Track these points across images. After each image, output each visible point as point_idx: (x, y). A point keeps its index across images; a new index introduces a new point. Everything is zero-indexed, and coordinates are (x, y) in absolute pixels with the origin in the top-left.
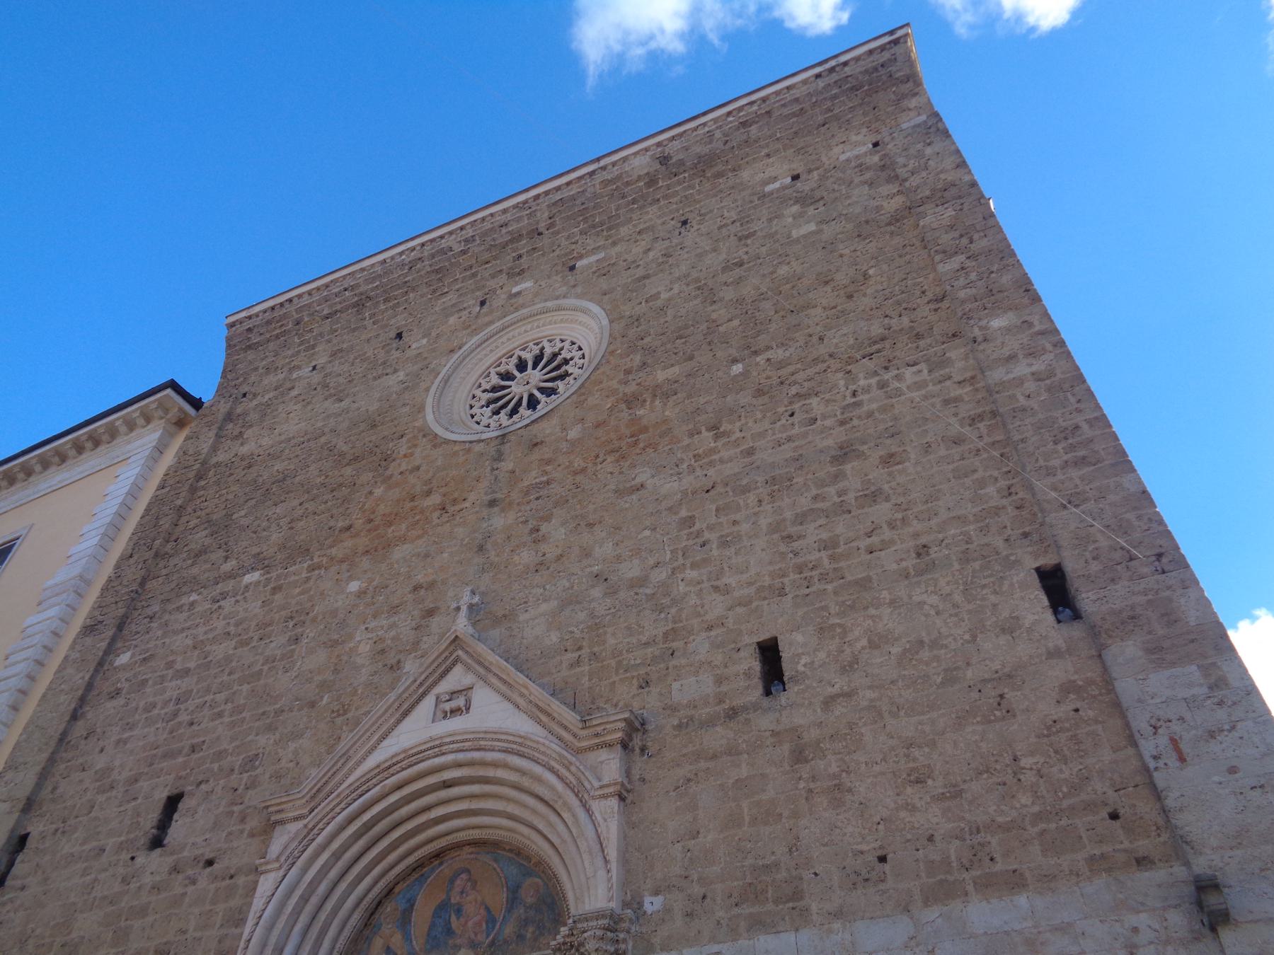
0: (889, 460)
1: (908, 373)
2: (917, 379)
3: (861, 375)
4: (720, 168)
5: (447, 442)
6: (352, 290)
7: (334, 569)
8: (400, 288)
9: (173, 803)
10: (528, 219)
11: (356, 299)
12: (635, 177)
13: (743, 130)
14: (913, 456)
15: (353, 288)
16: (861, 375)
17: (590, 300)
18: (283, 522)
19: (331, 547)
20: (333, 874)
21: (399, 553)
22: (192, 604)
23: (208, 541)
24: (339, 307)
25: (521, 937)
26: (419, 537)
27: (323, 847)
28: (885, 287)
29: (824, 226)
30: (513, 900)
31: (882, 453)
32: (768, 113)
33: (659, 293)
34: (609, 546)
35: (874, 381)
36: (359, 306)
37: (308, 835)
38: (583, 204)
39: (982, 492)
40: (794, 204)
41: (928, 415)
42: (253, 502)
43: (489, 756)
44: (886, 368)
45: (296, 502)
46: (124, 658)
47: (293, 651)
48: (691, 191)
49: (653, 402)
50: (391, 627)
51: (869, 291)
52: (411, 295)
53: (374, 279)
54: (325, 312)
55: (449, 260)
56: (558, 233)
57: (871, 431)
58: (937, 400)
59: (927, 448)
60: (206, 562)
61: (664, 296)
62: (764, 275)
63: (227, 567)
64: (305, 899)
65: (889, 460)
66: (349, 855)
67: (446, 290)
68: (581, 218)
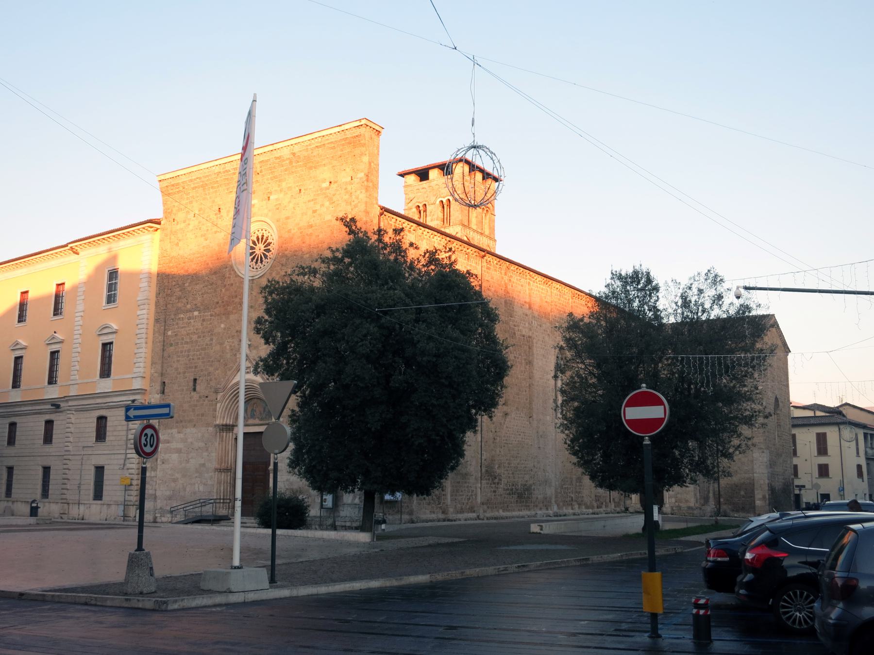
5: (239, 276)
7: (217, 317)
8: (215, 184)
9: (195, 380)
11: (202, 183)
12: (285, 158)
15: (200, 178)
17: (273, 222)
18: (200, 293)
19: (215, 309)
20: (231, 404)
21: (232, 317)
22: (183, 318)
24: (196, 185)
25: (266, 418)
26: (236, 313)
27: (227, 399)
30: (264, 411)
32: (324, 145)
33: (291, 229)
36: (204, 186)
37: (224, 396)
42: (189, 281)
43: (255, 385)
45: (202, 286)
46: (170, 333)
47: (212, 343)
50: (233, 342)
52: (220, 188)
53: (205, 177)
54: (192, 186)
55: (230, 175)
56: (263, 176)
60: (182, 302)
61: (293, 231)
63: (189, 306)
64: (226, 408)
66: (233, 400)
68: (270, 171)
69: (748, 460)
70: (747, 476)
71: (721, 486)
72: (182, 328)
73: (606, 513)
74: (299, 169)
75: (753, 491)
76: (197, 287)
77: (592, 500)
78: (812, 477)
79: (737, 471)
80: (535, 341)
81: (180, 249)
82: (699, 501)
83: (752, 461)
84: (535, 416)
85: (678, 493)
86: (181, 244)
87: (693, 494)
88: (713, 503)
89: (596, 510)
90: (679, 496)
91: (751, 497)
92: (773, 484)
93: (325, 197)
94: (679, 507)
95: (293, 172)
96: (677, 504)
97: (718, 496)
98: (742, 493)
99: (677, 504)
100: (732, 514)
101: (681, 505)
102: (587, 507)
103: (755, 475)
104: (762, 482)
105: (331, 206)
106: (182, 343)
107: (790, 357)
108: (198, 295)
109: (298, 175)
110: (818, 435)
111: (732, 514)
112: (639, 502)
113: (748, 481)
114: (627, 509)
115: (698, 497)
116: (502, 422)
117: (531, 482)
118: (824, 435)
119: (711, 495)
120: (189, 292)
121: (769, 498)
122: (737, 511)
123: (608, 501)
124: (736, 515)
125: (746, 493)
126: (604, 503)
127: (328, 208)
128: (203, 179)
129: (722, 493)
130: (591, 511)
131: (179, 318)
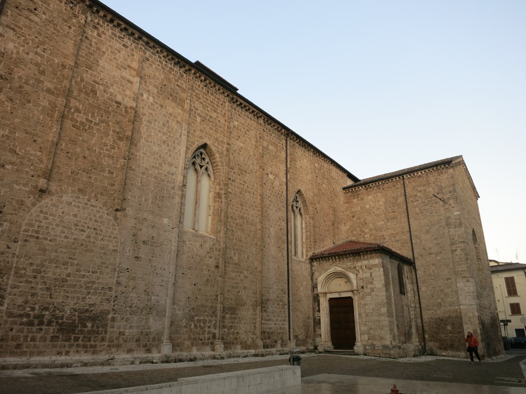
69: (452, 291)
70: (452, 308)
71: (424, 321)
73: (280, 354)
75: (461, 325)
77: (256, 338)
78: (506, 315)
79: (440, 303)
80: (145, 118)
82: (397, 338)
83: (457, 292)
84: (130, 211)
85: (371, 329)
87: (388, 328)
88: (417, 340)
89: (261, 350)
90: (372, 332)
91: (460, 332)
92: (482, 317)
94: (373, 346)
96: (370, 342)
97: (421, 331)
98: (449, 328)
99: (370, 342)
100: (439, 352)
101: (375, 343)
102: (246, 346)
103: (461, 307)
104: (471, 315)
107: (479, 201)
110: (507, 279)
111: (439, 352)
112: (330, 339)
113: (455, 314)
114: (316, 348)
115: (396, 334)
116: (28, 202)
117: (106, 307)
118: (512, 279)
119: (414, 330)
121: (481, 334)
122: (445, 349)
123: (286, 337)
124: (444, 354)
125: (453, 328)
126: (279, 342)
129: (426, 328)
130: (253, 351)
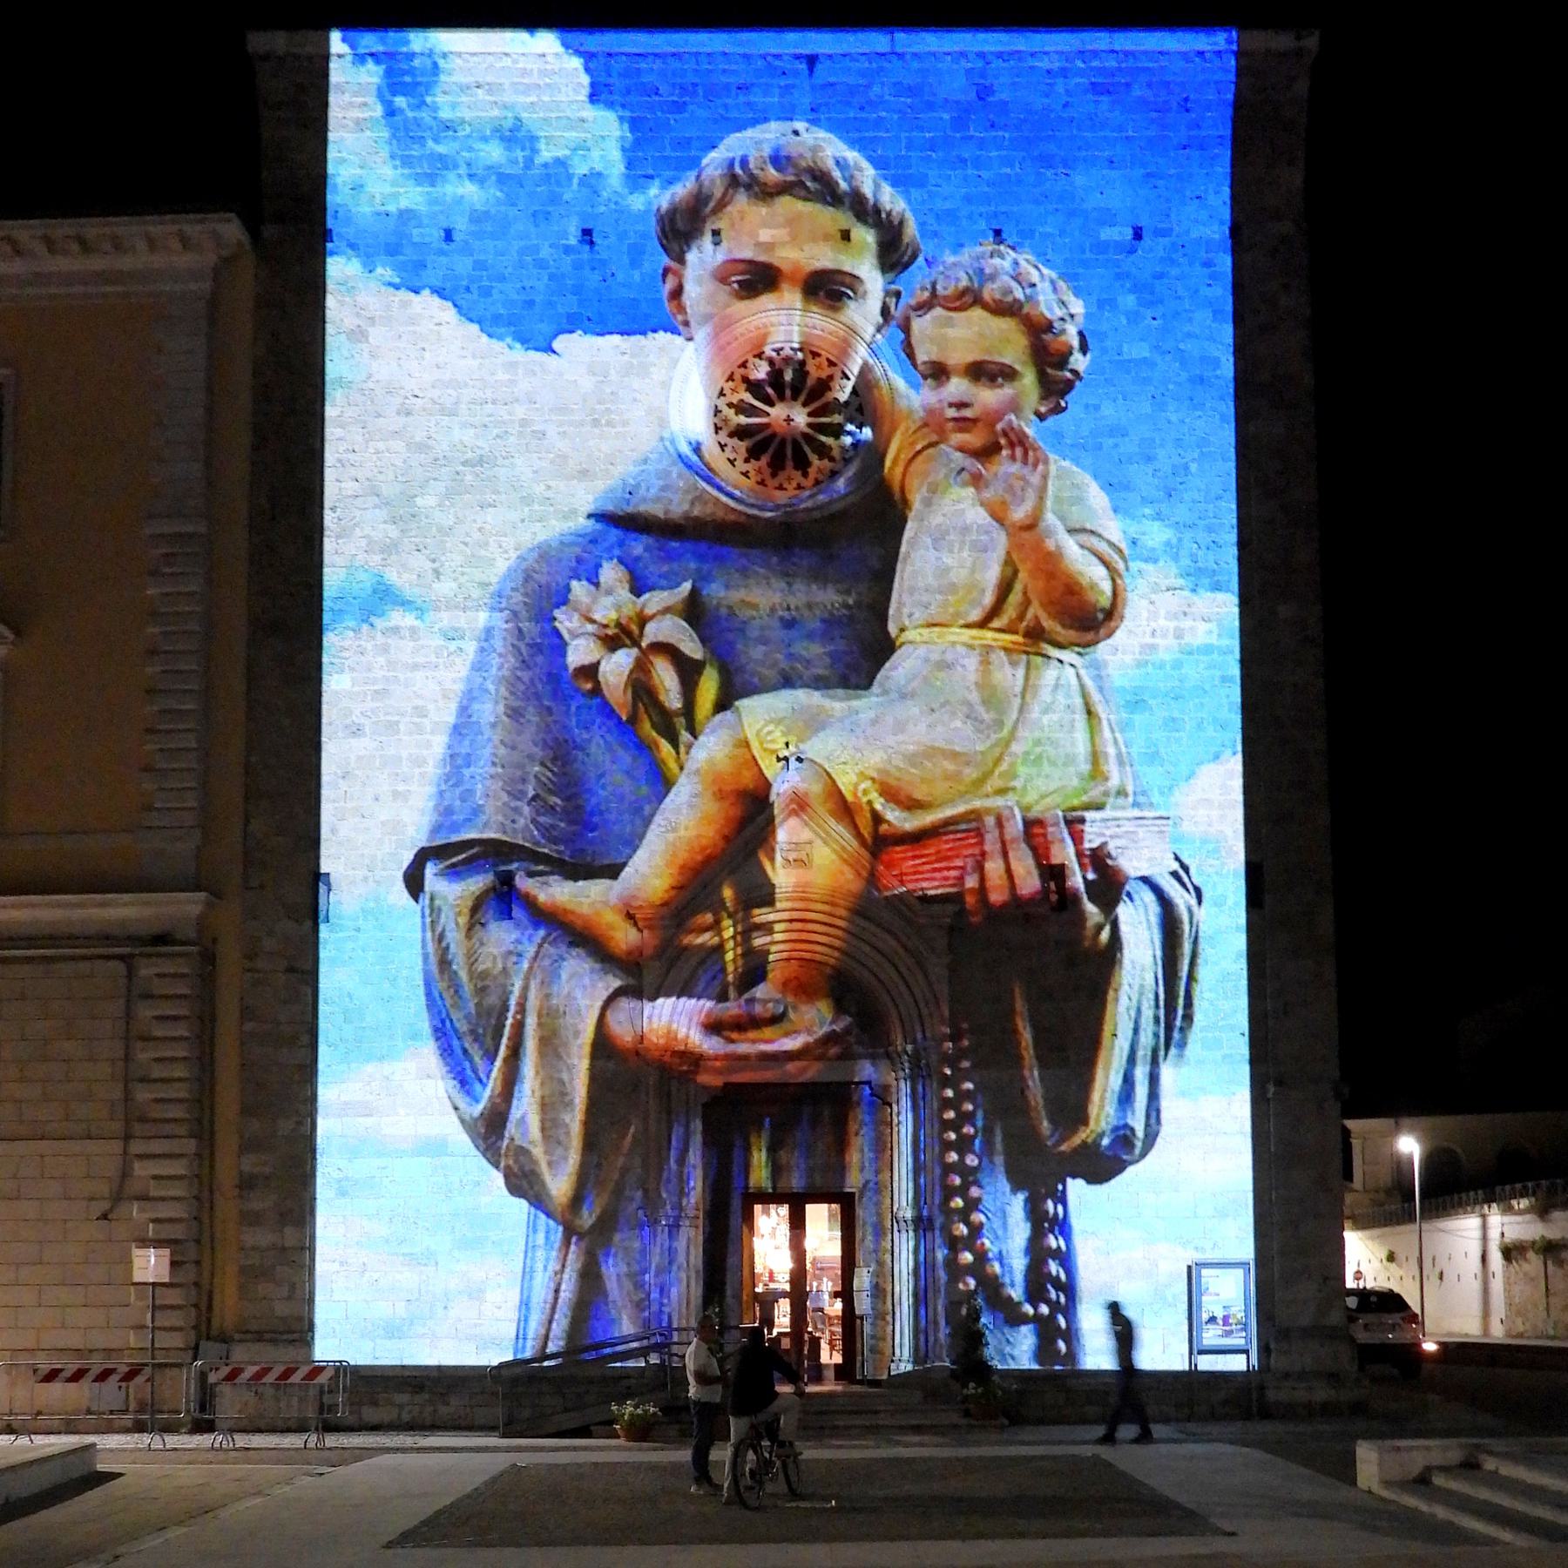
0: (1172, 724)
1: (1202, 627)
2: (1208, 641)
3: (1162, 612)
4: (1051, 148)
6: (490, 92)
8: (572, 128)
10: (781, 96)
13: (1090, 96)
14: (1188, 727)
16: (1162, 612)
23: (393, 532)
28: (1202, 499)
29: (1158, 359)
31: (1167, 714)
34: (922, 727)
35: (1172, 625)
38: (862, 108)
39: (1229, 783)
40: (1131, 291)
41: (1207, 687)
44: (1185, 614)
45: (514, 516)
48: (1008, 170)
49: (961, 550)
51: (1185, 496)
57: (1161, 685)
58: (1218, 673)
59: (1200, 726)
62: (1087, 406)
63: (445, 587)
65: (1172, 724)
67: (651, 172)
68: (857, 135)
72: (415, 667)
74: (994, 154)
76: (490, 516)
81: (373, 356)
86: (376, 334)
93: (1118, 276)
95: (964, 161)
105: (1149, 313)
106: (419, 729)
108: (493, 546)
109: (985, 174)
120: (447, 531)
127: (1134, 318)
128: (508, 97)
131: (396, 630)
